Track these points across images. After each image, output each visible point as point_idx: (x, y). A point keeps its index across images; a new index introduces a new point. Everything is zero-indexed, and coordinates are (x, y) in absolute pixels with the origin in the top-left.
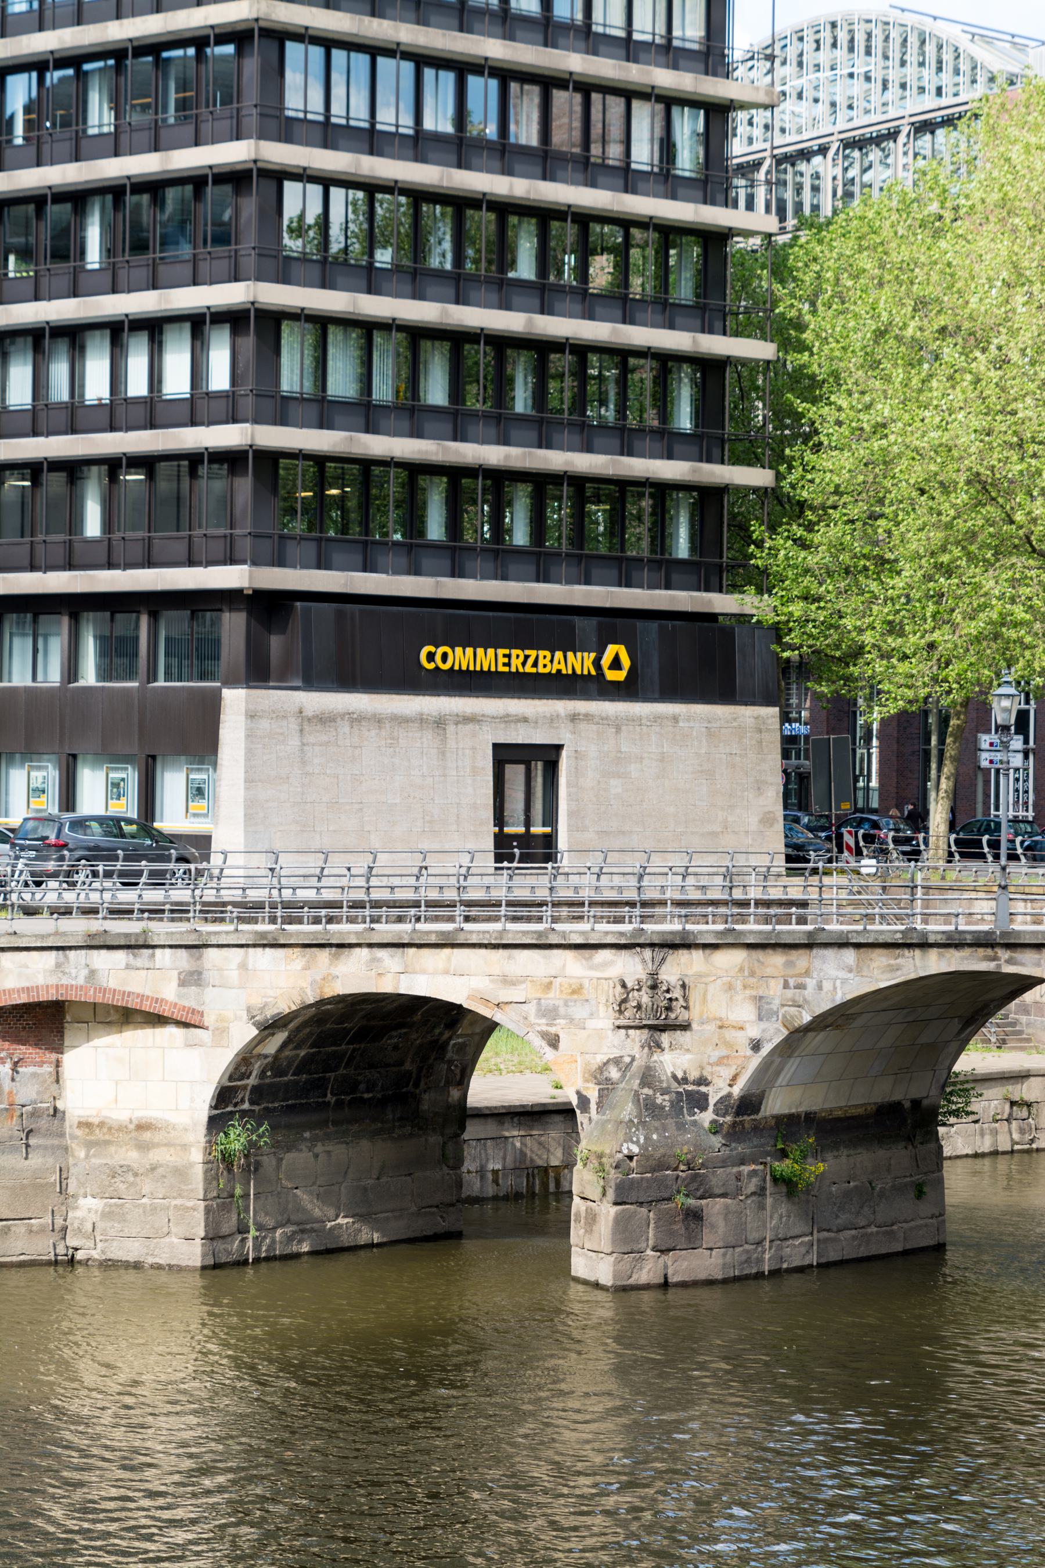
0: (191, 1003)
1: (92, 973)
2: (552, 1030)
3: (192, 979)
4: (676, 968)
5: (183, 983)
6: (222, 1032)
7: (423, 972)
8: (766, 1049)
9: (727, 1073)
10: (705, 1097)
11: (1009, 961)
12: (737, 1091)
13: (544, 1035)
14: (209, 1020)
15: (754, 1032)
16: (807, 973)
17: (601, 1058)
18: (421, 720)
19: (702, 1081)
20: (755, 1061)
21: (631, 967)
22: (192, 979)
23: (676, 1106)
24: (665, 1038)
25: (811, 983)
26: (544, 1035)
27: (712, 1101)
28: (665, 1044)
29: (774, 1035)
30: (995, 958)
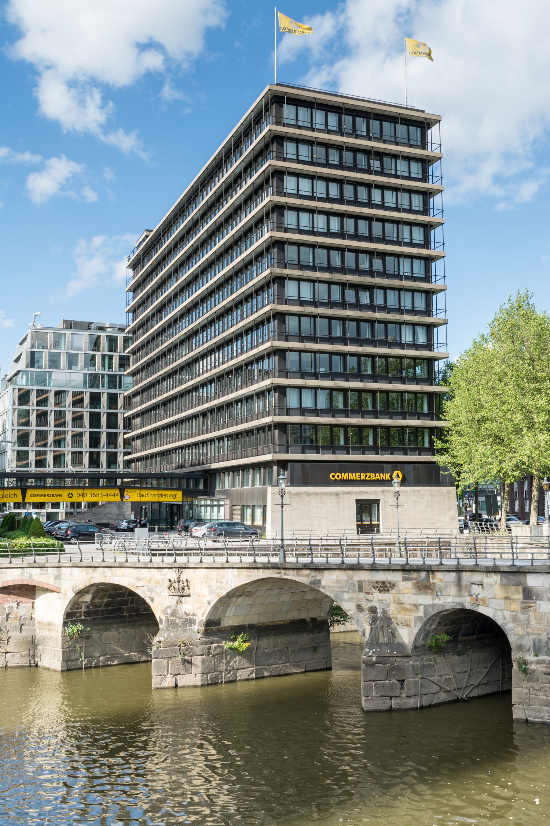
0: (57, 585)
1: (31, 576)
2: (152, 596)
3: (58, 577)
4: (186, 575)
5: (55, 579)
6: (65, 594)
7: (116, 576)
8: (212, 604)
9: (201, 612)
10: (195, 620)
11: (285, 574)
12: (204, 619)
13: (150, 597)
14: (62, 591)
15: (209, 598)
16: (223, 578)
17: (165, 606)
18: (331, 494)
19: (194, 615)
20: (209, 608)
21: (172, 575)
22: (58, 577)
23: (184, 624)
24: (183, 599)
25: (224, 581)
26: (150, 597)
27: (197, 622)
28: (183, 602)
29: (214, 599)
30: (280, 573)
